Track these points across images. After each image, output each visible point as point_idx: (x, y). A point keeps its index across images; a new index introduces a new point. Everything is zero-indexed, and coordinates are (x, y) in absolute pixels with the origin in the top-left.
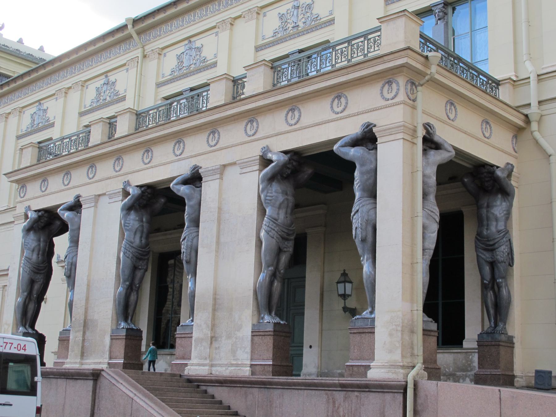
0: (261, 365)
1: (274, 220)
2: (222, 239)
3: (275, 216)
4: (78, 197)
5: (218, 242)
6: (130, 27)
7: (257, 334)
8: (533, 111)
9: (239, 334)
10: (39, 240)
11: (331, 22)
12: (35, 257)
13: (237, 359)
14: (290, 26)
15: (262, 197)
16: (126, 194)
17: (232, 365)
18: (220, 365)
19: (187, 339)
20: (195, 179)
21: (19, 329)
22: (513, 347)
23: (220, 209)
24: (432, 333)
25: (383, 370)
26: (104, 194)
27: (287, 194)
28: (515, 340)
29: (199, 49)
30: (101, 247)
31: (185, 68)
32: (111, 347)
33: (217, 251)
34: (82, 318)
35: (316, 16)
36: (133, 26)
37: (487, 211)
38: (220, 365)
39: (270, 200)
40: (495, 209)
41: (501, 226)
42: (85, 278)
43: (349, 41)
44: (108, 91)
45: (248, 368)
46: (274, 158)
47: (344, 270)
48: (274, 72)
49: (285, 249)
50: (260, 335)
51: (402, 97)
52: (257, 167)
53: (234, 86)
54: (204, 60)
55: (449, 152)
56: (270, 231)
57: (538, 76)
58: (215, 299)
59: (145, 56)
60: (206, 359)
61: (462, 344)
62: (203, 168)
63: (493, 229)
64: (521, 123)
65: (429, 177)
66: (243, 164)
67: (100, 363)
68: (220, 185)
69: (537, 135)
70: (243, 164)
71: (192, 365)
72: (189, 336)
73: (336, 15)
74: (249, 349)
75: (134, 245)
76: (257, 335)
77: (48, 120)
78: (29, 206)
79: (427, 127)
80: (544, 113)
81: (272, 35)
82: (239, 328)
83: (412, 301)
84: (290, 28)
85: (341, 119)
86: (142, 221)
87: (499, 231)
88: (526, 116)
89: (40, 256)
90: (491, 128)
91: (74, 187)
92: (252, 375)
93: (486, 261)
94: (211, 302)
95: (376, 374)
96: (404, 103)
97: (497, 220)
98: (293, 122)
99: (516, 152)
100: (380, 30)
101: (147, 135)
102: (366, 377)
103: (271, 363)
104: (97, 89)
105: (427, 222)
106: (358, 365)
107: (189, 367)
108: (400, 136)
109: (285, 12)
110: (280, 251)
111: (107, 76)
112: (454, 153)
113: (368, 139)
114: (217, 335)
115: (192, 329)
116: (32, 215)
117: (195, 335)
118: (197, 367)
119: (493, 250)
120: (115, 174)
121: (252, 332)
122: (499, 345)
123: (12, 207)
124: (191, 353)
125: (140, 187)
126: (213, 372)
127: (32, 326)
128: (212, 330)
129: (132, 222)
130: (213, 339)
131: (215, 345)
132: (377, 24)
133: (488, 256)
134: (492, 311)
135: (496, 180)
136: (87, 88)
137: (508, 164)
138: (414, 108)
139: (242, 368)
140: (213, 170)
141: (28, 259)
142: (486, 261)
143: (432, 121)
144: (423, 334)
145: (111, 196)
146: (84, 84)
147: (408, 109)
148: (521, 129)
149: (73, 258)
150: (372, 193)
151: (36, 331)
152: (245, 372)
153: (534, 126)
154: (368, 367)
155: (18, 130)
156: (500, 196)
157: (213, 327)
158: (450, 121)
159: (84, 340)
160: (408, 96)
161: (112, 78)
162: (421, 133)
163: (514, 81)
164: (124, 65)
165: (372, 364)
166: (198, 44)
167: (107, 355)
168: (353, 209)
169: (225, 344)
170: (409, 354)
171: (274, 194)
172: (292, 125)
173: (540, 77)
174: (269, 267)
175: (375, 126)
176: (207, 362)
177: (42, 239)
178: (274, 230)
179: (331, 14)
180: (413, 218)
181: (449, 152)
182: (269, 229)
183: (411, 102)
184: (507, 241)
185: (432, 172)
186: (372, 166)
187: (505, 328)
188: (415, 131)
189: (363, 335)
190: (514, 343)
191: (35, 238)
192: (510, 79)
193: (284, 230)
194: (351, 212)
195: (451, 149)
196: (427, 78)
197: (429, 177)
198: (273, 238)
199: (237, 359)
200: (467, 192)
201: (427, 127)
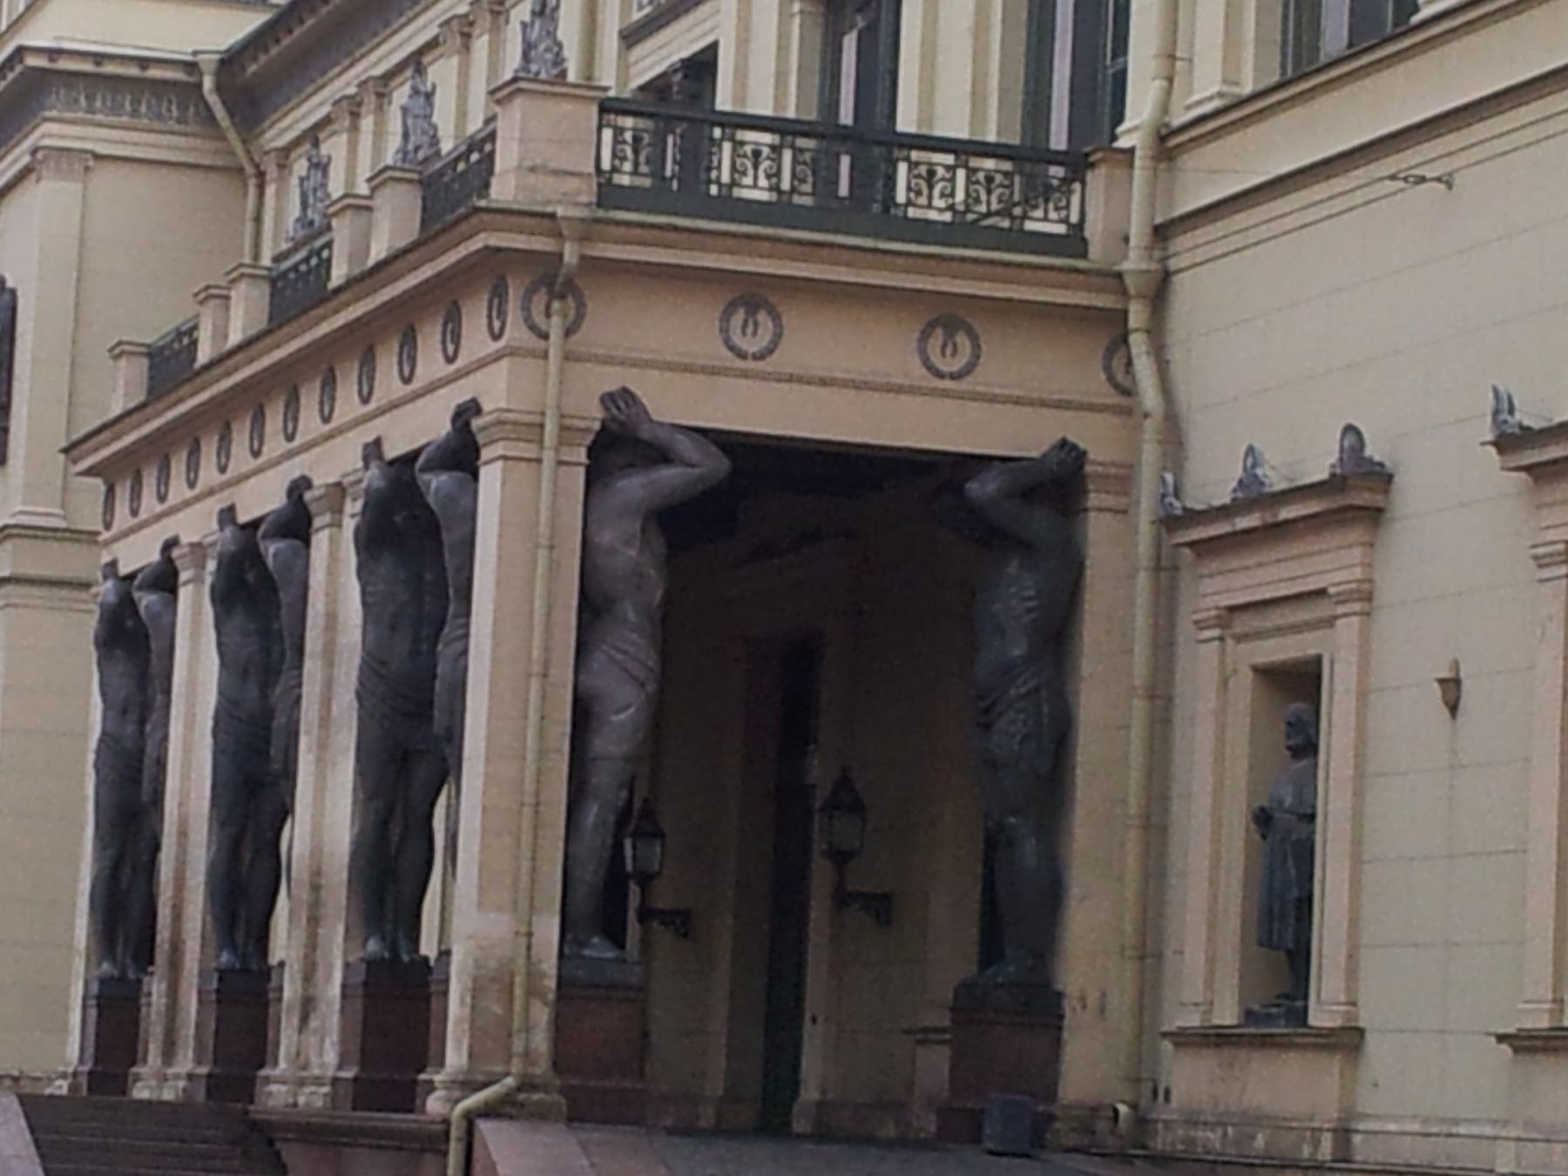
4: (170, 545)
28: (1067, 1006)
55: (692, 466)
96: (510, 352)
99: (1126, 392)
131: (314, 1023)
153: (1137, 315)
171: (381, 587)
201: (619, 399)
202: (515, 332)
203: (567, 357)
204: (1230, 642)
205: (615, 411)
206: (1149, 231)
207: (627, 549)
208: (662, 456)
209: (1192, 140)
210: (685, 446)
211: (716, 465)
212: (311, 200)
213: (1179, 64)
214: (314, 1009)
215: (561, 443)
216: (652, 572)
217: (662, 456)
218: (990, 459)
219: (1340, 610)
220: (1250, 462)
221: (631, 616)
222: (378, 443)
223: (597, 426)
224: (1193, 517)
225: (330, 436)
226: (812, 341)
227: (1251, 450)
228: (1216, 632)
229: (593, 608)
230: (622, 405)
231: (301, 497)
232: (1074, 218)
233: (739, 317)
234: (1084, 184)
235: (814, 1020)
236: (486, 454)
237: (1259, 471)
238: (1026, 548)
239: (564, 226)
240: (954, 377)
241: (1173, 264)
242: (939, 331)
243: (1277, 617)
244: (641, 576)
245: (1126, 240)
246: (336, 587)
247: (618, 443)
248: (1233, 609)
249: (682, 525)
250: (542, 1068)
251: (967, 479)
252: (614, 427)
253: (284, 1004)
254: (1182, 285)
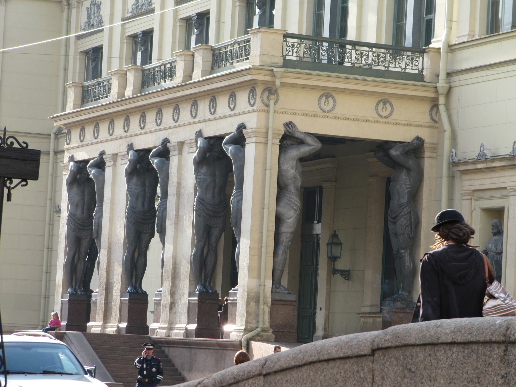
2: (180, 213)
4: (102, 153)
12: (79, 212)
24: (294, 303)
34: (105, 281)
47: (335, 231)
55: (311, 145)
89: (85, 211)
96: (257, 110)
99: (435, 122)
108: (254, 139)
112: (316, 145)
113: (239, 140)
119: (395, 223)
131: (174, 310)
147: (263, 115)
153: (442, 100)
170: (254, 321)
171: (202, 176)
177: (86, 193)
181: (311, 145)
201: (289, 125)
202: (259, 104)
203: (275, 112)
204: (473, 201)
205: (288, 128)
206: (445, 74)
207: (291, 170)
208: (301, 142)
209: (459, 48)
210: (309, 140)
211: (316, 145)
212: (92, 16)
213: (454, 23)
214: (174, 306)
215: (273, 138)
216: (299, 177)
217: (301, 142)
218: (395, 142)
219: (511, 194)
220: (482, 148)
221: (293, 191)
222: (200, 132)
223: (283, 133)
224: (459, 163)
225: (177, 127)
226: (345, 105)
227: (482, 145)
228: (469, 197)
229: (281, 188)
230: (291, 127)
231: (166, 145)
232: (420, 69)
233: (324, 99)
234: (423, 58)
235: (321, 309)
236: (247, 141)
237: (485, 152)
238: (408, 170)
239: (276, 74)
240: (386, 117)
241: (452, 84)
242: (381, 104)
243: (488, 194)
244: (295, 178)
245: (438, 76)
246: (184, 176)
247: (289, 139)
248: (474, 191)
250: (267, 325)
251: (390, 148)
252: (287, 133)
254: (456, 92)
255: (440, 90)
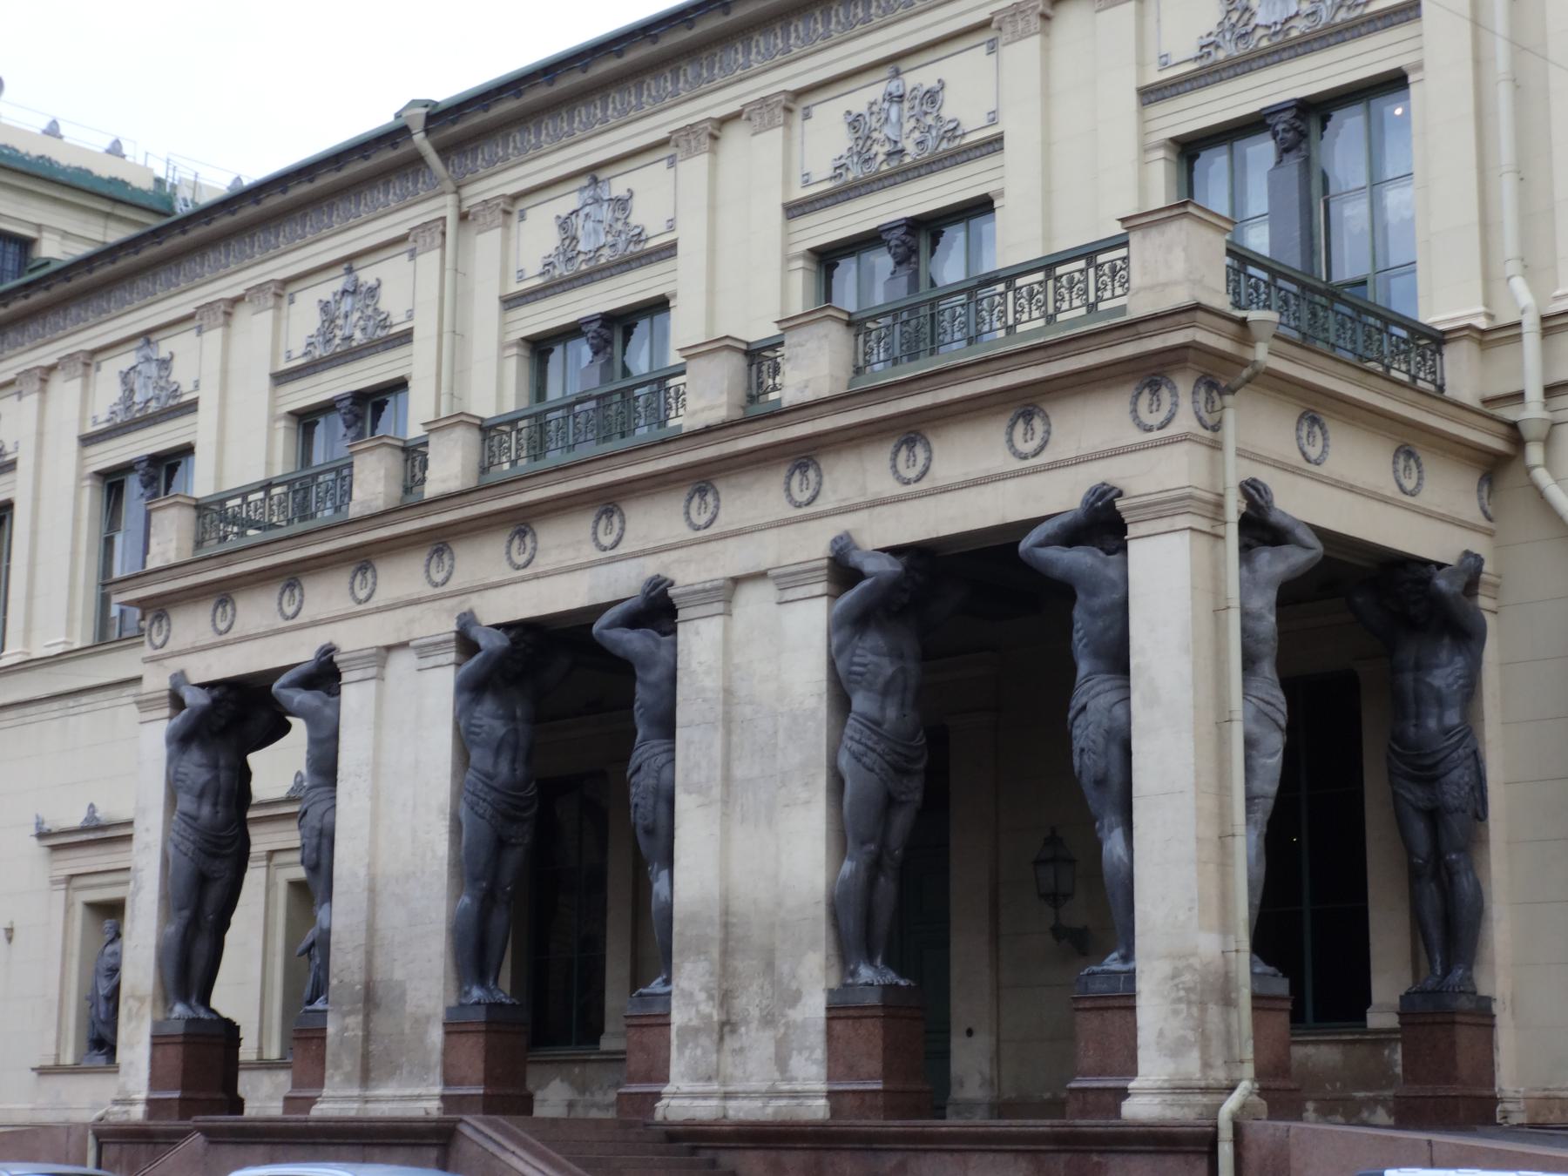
0: (854, 1092)
1: (874, 724)
2: (739, 771)
3: (875, 714)
4: (328, 652)
5: (727, 779)
6: (419, 138)
7: (842, 1013)
8: (1533, 411)
9: (795, 1015)
10: (214, 766)
11: (994, 144)
13: (791, 1080)
14: (880, 150)
15: (840, 665)
16: (466, 643)
17: (779, 1095)
18: (748, 1095)
19: (657, 1030)
20: (658, 610)
21: (171, 1010)
22: (1492, 1026)
23: (728, 692)
24: (1279, 1004)
25: (1157, 1100)
26: (404, 645)
27: (901, 657)
28: (1497, 1008)
29: (622, 204)
30: (399, 788)
31: (582, 257)
32: (446, 1051)
33: (726, 802)
35: (952, 126)
36: (427, 131)
37: (1416, 680)
38: (748, 1095)
39: (861, 674)
40: (1438, 672)
41: (1452, 718)
42: (362, 872)
43: (1048, 265)
44: (357, 315)
45: (822, 1102)
46: (870, 566)
48: (857, 336)
49: (903, 797)
50: (848, 1018)
51: (1185, 421)
52: (821, 588)
53: (750, 366)
54: (639, 238)
55: (1309, 548)
56: (865, 755)
57: (1544, 319)
58: (726, 926)
59: (463, 217)
60: (709, 1079)
61: (1364, 1019)
62: (678, 583)
63: (1432, 723)
64: (1498, 444)
65: (1260, 617)
66: (786, 580)
67: (419, 1098)
68: (726, 630)
69: (1542, 476)
70: (786, 580)
71: (674, 1095)
72: (661, 1021)
73: (1007, 126)
74: (820, 1053)
75: (495, 784)
76: (840, 1018)
77: (176, 393)
78: (182, 673)
79: (1253, 492)
80: (1560, 416)
81: (830, 173)
82: (795, 998)
83: (1225, 929)
84: (881, 157)
85: (1035, 471)
86: (513, 718)
87: (1447, 732)
88: (1514, 426)
90: (1419, 465)
91: (314, 624)
92: (832, 1116)
93: (1418, 810)
94: (715, 932)
95: (1140, 1108)
97: (1441, 702)
98: (912, 473)
99: (1490, 519)
100: (1126, 244)
101: (520, 492)
102: (1118, 1114)
103: (880, 1087)
104: (325, 307)
105: (1256, 730)
106: (1098, 1089)
107: (664, 1102)
108: (1182, 521)
109: (863, 109)
110: (890, 802)
111: (350, 271)
112: (1318, 548)
113: (1103, 524)
114: (734, 1018)
115: (668, 1004)
116: (196, 699)
117: (678, 1017)
118: (686, 1102)
120: (430, 591)
121: (828, 1009)
122: (1454, 1023)
123: (77, 646)
124: (668, 1067)
125: (506, 627)
126: (731, 1113)
127: (205, 999)
128: (721, 1005)
129: (486, 721)
130: (727, 1026)
131: (730, 1043)
132: (1118, 229)
133: (1419, 793)
134: (1435, 934)
135: (1437, 601)
136: (292, 302)
137: (1467, 554)
138: (1216, 446)
139: (809, 1102)
140: (705, 591)
141: (190, 819)
142: (1418, 810)
143: (1264, 475)
144: (1254, 1009)
145: (426, 650)
146: (283, 289)
147: (1202, 452)
148: (1498, 464)
149: (323, 815)
150: (1117, 660)
151: (213, 1011)
152: (818, 1109)
153: (1534, 454)
154: (1124, 1093)
155: (82, 419)
156: (1447, 641)
157: (725, 998)
158: (1308, 468)
159: (367, 1038)
160: (1200, 419)
161: (367, 276)
162: (1234, 507)
163: (1483, 332)
164: (402, 240)
165: (1131, 1085)
166: (618, 187)
167: (437, 1074)
168: (1073, 703)
169: (757, 1044)
171: (870, 658)
172: (908, 483)
173: (1550, 325)
174: (863, 843)
175: (1120, 494)
176: (715, 1087)
177: (222, 762)
178: (873, 750)
179: (993, 122)
180: (1222, 722)
181: (1309, 548)
182: (862, 748)
183: (1208, 434)
184: (1467, 757)
185: (1264, 602)
186: (1116, 596)
187: (1470, 978)
188: (1219, 506)
189: (1108, 1014)
190: (1493, 1016)
191: (204, 761)
192: (1469, 327)
193: (899, 749)
194: (1068, 710)
195: (1311, 540)
196: (1246, 373)
197: (1260, 617)
198: (871, 770)
199: (791, 1080)
200: (1359, 653)
201: (1253, 492)
249: (1291, 595)
253: (674, 1028)
255: (1528, 432)
